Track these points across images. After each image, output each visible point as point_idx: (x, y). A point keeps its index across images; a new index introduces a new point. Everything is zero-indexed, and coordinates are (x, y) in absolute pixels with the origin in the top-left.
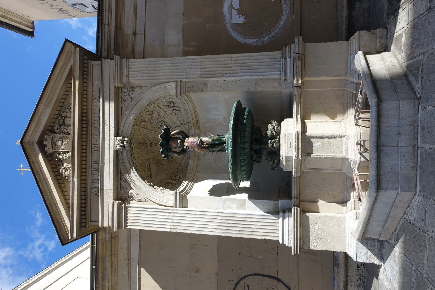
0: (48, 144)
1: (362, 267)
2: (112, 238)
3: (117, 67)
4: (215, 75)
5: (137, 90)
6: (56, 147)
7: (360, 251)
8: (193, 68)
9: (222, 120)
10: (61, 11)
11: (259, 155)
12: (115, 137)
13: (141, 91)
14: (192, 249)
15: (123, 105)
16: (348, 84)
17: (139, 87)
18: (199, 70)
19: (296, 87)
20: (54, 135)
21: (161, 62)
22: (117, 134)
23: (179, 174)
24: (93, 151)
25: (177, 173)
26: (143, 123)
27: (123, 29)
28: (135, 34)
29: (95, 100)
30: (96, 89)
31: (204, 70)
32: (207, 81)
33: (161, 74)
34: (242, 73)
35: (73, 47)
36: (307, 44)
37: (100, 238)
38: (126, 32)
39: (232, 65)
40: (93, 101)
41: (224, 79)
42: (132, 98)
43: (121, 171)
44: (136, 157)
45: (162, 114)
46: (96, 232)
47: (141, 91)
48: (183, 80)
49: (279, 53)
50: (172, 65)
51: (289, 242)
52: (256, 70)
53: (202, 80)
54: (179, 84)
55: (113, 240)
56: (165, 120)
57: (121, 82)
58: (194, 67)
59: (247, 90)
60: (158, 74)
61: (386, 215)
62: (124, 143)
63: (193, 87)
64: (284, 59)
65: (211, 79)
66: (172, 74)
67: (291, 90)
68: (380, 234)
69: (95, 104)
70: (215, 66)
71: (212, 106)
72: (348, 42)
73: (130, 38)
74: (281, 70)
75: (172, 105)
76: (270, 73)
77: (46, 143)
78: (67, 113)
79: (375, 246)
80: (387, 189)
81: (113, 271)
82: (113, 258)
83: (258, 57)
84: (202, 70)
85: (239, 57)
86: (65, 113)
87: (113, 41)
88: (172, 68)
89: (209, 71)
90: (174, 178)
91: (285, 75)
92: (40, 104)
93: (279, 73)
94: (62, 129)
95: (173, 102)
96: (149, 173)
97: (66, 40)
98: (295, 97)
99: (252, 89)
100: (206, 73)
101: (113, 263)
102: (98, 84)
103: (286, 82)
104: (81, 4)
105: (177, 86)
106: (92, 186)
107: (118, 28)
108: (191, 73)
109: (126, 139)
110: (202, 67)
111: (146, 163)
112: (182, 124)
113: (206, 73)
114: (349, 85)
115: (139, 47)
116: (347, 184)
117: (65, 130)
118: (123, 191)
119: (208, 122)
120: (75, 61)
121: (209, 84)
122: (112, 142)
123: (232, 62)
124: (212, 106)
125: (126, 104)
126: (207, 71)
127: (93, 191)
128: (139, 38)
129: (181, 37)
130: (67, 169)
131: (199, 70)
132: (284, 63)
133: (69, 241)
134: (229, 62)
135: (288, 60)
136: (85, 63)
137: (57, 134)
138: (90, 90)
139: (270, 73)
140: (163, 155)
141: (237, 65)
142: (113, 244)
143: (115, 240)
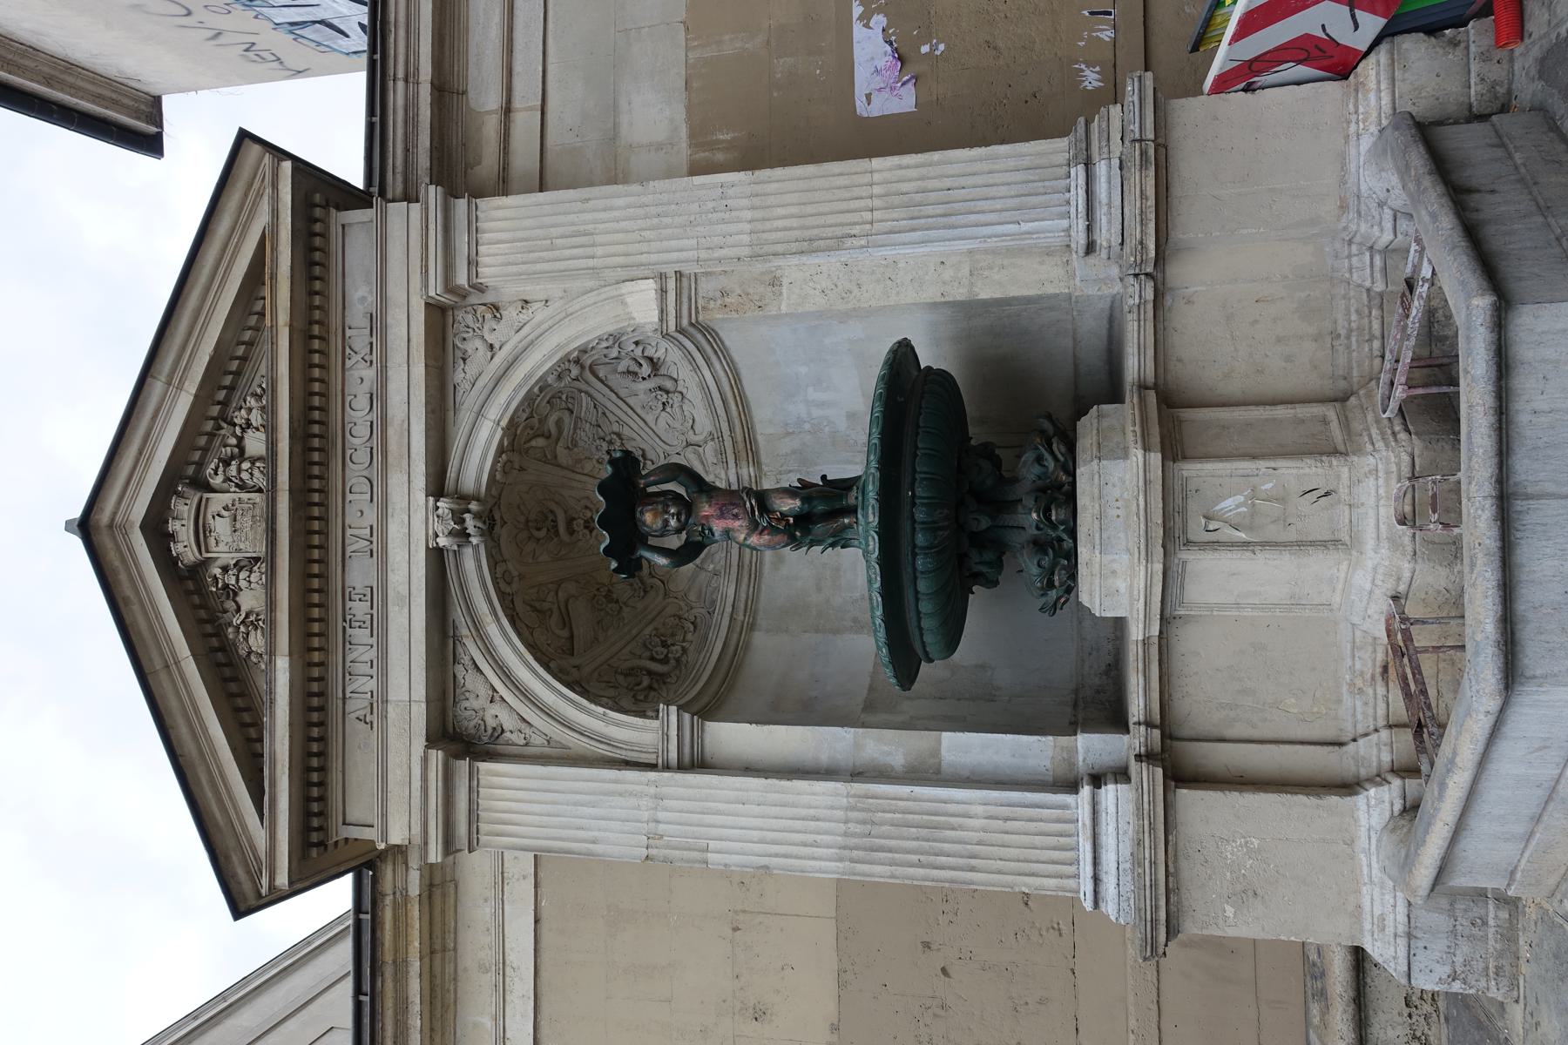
1: (1427, 1008)
2: (431, 885)
3: (432, 226)
4: (810, 246)
5: (511, 314)
6: (212, 542)
7: (1421, 944)
8: (724, 221)
9: (842, 425)
10: (251, 54)
11: (989, 556)
13: (523, 317)
14: (736, 929)
15: (458, 376)
16: (1349, 256)
17: (520, 304)
18: (747, 227)
19: (1136, 275)
20: (206, 495)
21: (601, 203)
22: (437, 488)
23: (679, 637)
24: (348, 554)
25: (673, 635)
26: (540, 442)
27: (464, 93)
28: (507, 110)
29: (355, 358)
30: (357, 316)
31: (768, 225)
32: (779, 267)
33: (600, 251)
34: (914, 230)
35: (267, 158)
36: (1177, 103)
37: (387, 885)
38: (473, 104)
39: (877, 203)
40: (349, 363)
41: (844, 256)
43: (455, 628)
44: (515, 573)
45: (609, 404)
46: (370, 865)
47: (523, 317)
48: (687, 269)
49: (1062, 143)
50: (641, 211)
51: (1124, 905)
52: (973, 218)
53: (759, 267)
55: (437, 892)
56: (626, 432)
57: (450, 287)
58: (727, 216)
59: (940, 299)
60: (589, 251)
61: (1541, 793)
62: (464, 521)
63: (724, 294)
64: (1081, 168)
65: (795, 260)
66: (644, 247)
67: (1117, 288)
68: (1512, 873)
70: (809, 209)
71: (803, 370)
72: (1344, 83)
73: (491, 127)
74: (1073, 210)
76: (1026, 227)
77: (173, 526)
78: (250, 410)
79: (1485, 923)
81: (438, 1013)
82: (437, 962)
83: (977, 167)
84: (759, 226)
85: (900, 167)
87: (424, 140)
88: (641, 223)
89: (785, 229)
90: (660, 652)
91: (1089, 229)
92: (149, 380)
93: (1065, 223)
94: (234, 473)
95: (651, 359)
96: (565, 633)
97: (244, 136)
98: (1130, 317)
99: (959, 294)
100: (774, 236)
101: (438, 981)
102: (363, 299)
103: (1092, 260)
104: (321, 22)
105: (663, 291)
106: (348, 690)
107: (447, 91)
109: (474, 506)
111: (550, 598)
112: (688, 444)
113: (774, 236)
114: (1354, 260)
115: (524, 155)
116: (1358, 666)
117: (245, 476)
119: (788, 434)
121: (785, 281)
122: (419, 517)
123: (877, 190)
124: (803, 370)
125: (472, 369)
126: (777, 230)
127: (350, 706)
129: (679, 112)
130: (251, 622)
131: (747, 227)
132: (1082, 180)
133: (262, 902)
134: (864, 192)
135: (1101, 169)
136: (316, 220)
137: (214, 491)
138: (335, 321)
139: (1026, 227)
140: (614, 565)
141: (897, 200)
142: (437, 911)
143: (444, 895)
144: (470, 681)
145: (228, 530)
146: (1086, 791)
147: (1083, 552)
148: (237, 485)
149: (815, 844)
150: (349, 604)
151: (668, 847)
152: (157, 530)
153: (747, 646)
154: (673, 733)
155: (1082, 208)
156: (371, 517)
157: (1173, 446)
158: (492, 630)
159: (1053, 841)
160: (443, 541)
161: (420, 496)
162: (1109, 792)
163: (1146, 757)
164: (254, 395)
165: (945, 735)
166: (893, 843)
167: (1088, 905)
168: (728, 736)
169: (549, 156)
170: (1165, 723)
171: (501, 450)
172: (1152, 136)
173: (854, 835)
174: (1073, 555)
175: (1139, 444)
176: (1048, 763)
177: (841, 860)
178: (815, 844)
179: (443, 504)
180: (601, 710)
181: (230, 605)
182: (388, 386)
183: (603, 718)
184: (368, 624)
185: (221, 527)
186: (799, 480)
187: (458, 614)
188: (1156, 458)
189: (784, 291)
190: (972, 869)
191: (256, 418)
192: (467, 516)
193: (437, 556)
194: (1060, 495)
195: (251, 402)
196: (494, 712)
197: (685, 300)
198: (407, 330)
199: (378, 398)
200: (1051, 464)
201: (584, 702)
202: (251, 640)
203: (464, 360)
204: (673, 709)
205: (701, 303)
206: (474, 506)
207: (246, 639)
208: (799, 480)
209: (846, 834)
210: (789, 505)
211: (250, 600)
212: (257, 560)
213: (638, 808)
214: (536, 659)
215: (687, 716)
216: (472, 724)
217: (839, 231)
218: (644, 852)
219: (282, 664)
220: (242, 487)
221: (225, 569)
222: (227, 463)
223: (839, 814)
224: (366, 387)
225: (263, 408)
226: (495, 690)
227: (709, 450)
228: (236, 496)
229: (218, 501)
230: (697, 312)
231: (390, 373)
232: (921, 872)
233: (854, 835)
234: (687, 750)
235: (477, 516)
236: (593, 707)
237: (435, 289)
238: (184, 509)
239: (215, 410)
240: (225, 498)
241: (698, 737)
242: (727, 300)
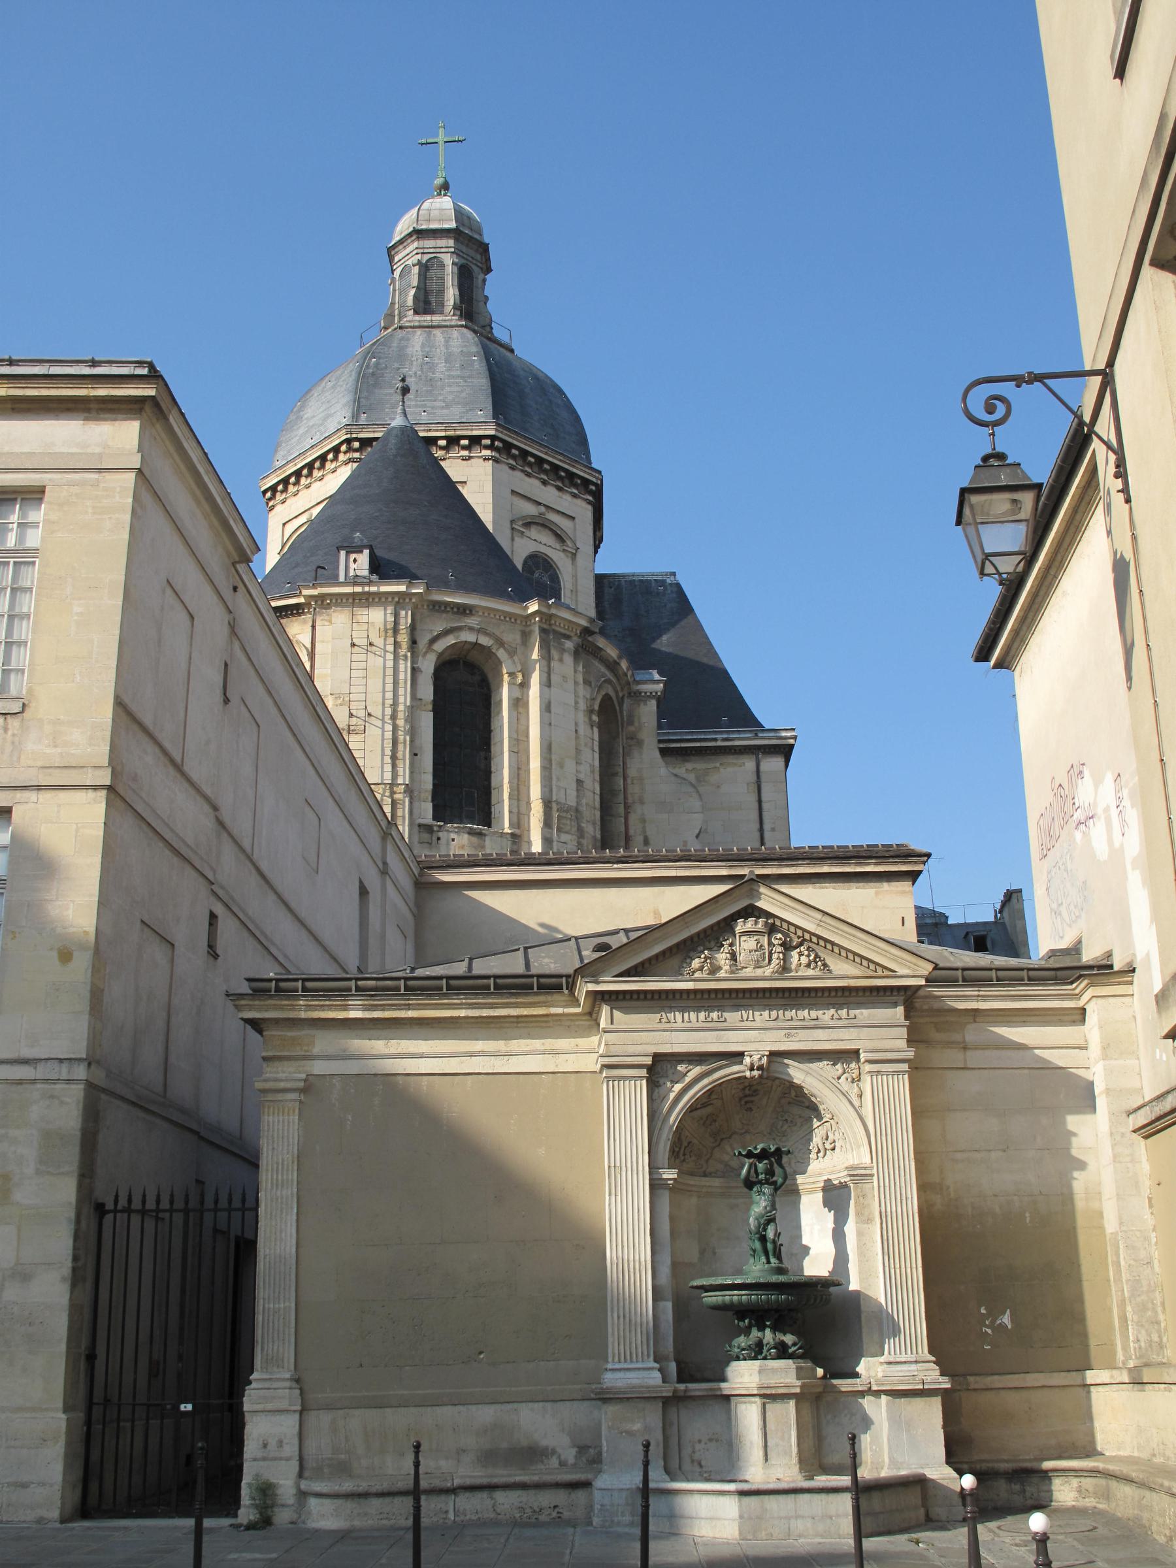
0: (750, 924)
1: (554, 1514)
22: (773, 1054)
36: (939, 1399)
38: (969, 1026)
42: (839, 1078)
48: (875, 1178)
75: (828, 1146)
78: (808, 956)
80: (740, 1506)
86: (806, 953)
105: (865, 1168)
128: (953, 1057)
135: (913, 1367)
138: (851, 999)
146: (657, 1365)
147: (757, 1363)
156: (758, 1023)
158: (706, 1081)
160: (747, 1060)
162: (658, 1375)
163: (675, 1391)
167: (610, 1366)
169: (940, 1072)
174: (755, 1358)
181: (713, 944)
188: (798, 1390)
191: (804, 960)
193: (741, 1055)
194: (782, 1352)
200: (793, 1349)
204: (675, 1176)
210: (770, 1233)
219: (690, 986)
220: (770, 954)
221: (731, 945)
222: (781, 945)
225: (808, 966)
229: (765, 940)
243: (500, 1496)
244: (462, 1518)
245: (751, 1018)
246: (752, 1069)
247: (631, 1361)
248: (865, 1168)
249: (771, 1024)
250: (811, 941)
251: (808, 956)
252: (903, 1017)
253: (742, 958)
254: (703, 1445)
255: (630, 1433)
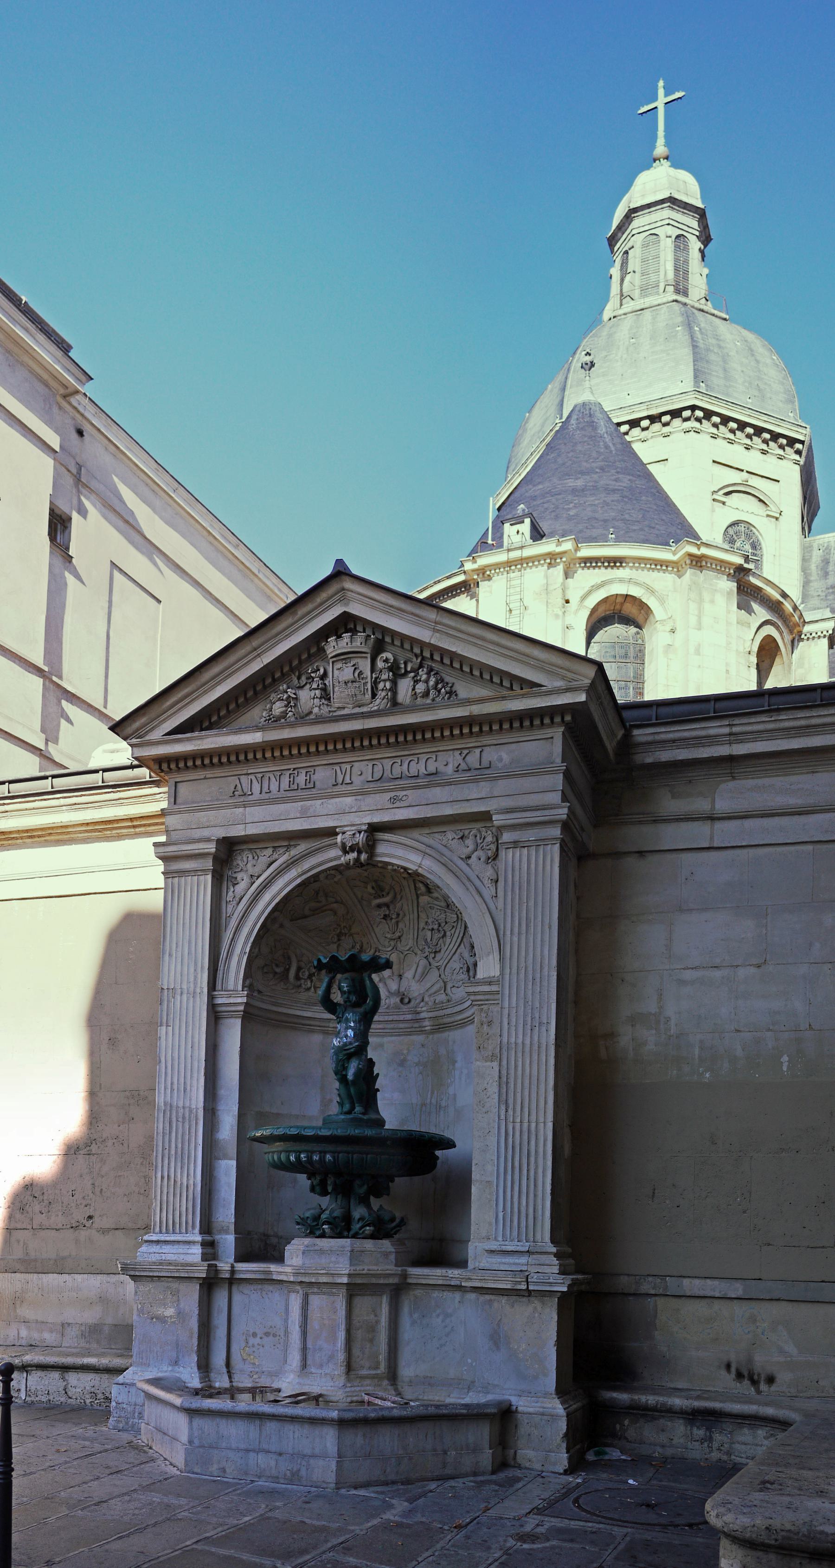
3: (538, 813)
4: (503, 1082)
12: (365, 827)
15: (450, 835)
17: (495, 877)
20: (369, 656)
22: (374, 829)
31: (520, 1055)
33: (515, 939)
39: (526, 1125)
40: (457, 753)
42: (469, 857)
43: (295, 846)
47: (486, 882)
54: (494, 988)
57: (500, 829)
60: (516, 930)
62: (353, 851)
63: (490, 1023)
66: (514, 970)
69: (450, 760)
96: (307, 912)
108: (514, 1020)
110: (527, 1049)
112: (445, 983)
118: (250, 857)
120: (550, 693)
123: (533, 1125)
125: (455, 844)
127: (244, 779)
131: (520, 1041)
135: (523, 1260)
141: (525, 1137)
144: (263, 860)
145: (346, 678)
148: (376, 678)
149: (172, 1090)
150: (304, 772)
151: (168, 1001)
152: (346, 624)
153: (313, 1031)
154: (232, 1000)
155: (504, 1248)
157: (354, 1290)
158: (293, 873)
159: (177, 1220)
161: (368, 819)
162: (197, 1250)
164: (437, 683)
165: (234, 1163)
166: (174, 1134)
167: (146, 1238)
168: (232, 1036)
170: (233, 1281)
171: (405, 869)
172: (531, 1288)
173: (177, 1112)
175: (352, 1272)
176: (220, 1219)
177: (165, 1104)
178: (172, 1090)
179: (361, 838)
180: (248, 950)
182: (439, 784)
183: (243, 952)
184: (293, 787)
185: (347, 673)
186: (378, 1075)
187: (302, 847)
188: (345, 1280)
189: (488, 1064)
190: (162, 1177)
191: (421, 688)
192: (355, 855)
193: (331, 832)
195: (432, 683)
196: (245, 878)
197: (487, 997)
198: (473, 798)
199: (433, 779)
201: (252, 939)
202: (278, 704)
203: (462, 838)
204: (245, 1000)
205: (485, 1007)
206: (364, 857)
207: (280, 699)
208: (378, 1075)
209: (177, 1107)
211: (307, 697)
212: (329, 699)
213: (188, 982)
214: (278, 904)
215: (242, 1008)
216: (240, 862)
217: (511, 1101)
218: (165, 987)
220: (375, 683)
221: (324, 676)
222: (390, 669)
223: (187, 1104)
224: (442, 768)
225: (426, 694)
226: (258, 877)
227: (442, 997)
228: (369, 679)
229: (365, 665)
230: (479, 1005)
231: (447, 787)
232: (160, 1149)
233: (177, 1112)
234: (224, 1009)
235: (357, 860)
236: (249, 945)
237: (498, 819)
238: (358, 642)
239: (427, 654)
240: (367, 672)
241: (232, 1015)
242: (485, 1026)
243: (73, 1378)
244: (33, 1399)
245: (347, 780)
246: (345, 852)
247: (174, 1232)
248: (490, 983)
249: (372, 785)
250: (432, 658)
251: (427, 682)
252: (559, 760)
253: (339, 695)
254: (257, 1340)
255: (162, 1319)
